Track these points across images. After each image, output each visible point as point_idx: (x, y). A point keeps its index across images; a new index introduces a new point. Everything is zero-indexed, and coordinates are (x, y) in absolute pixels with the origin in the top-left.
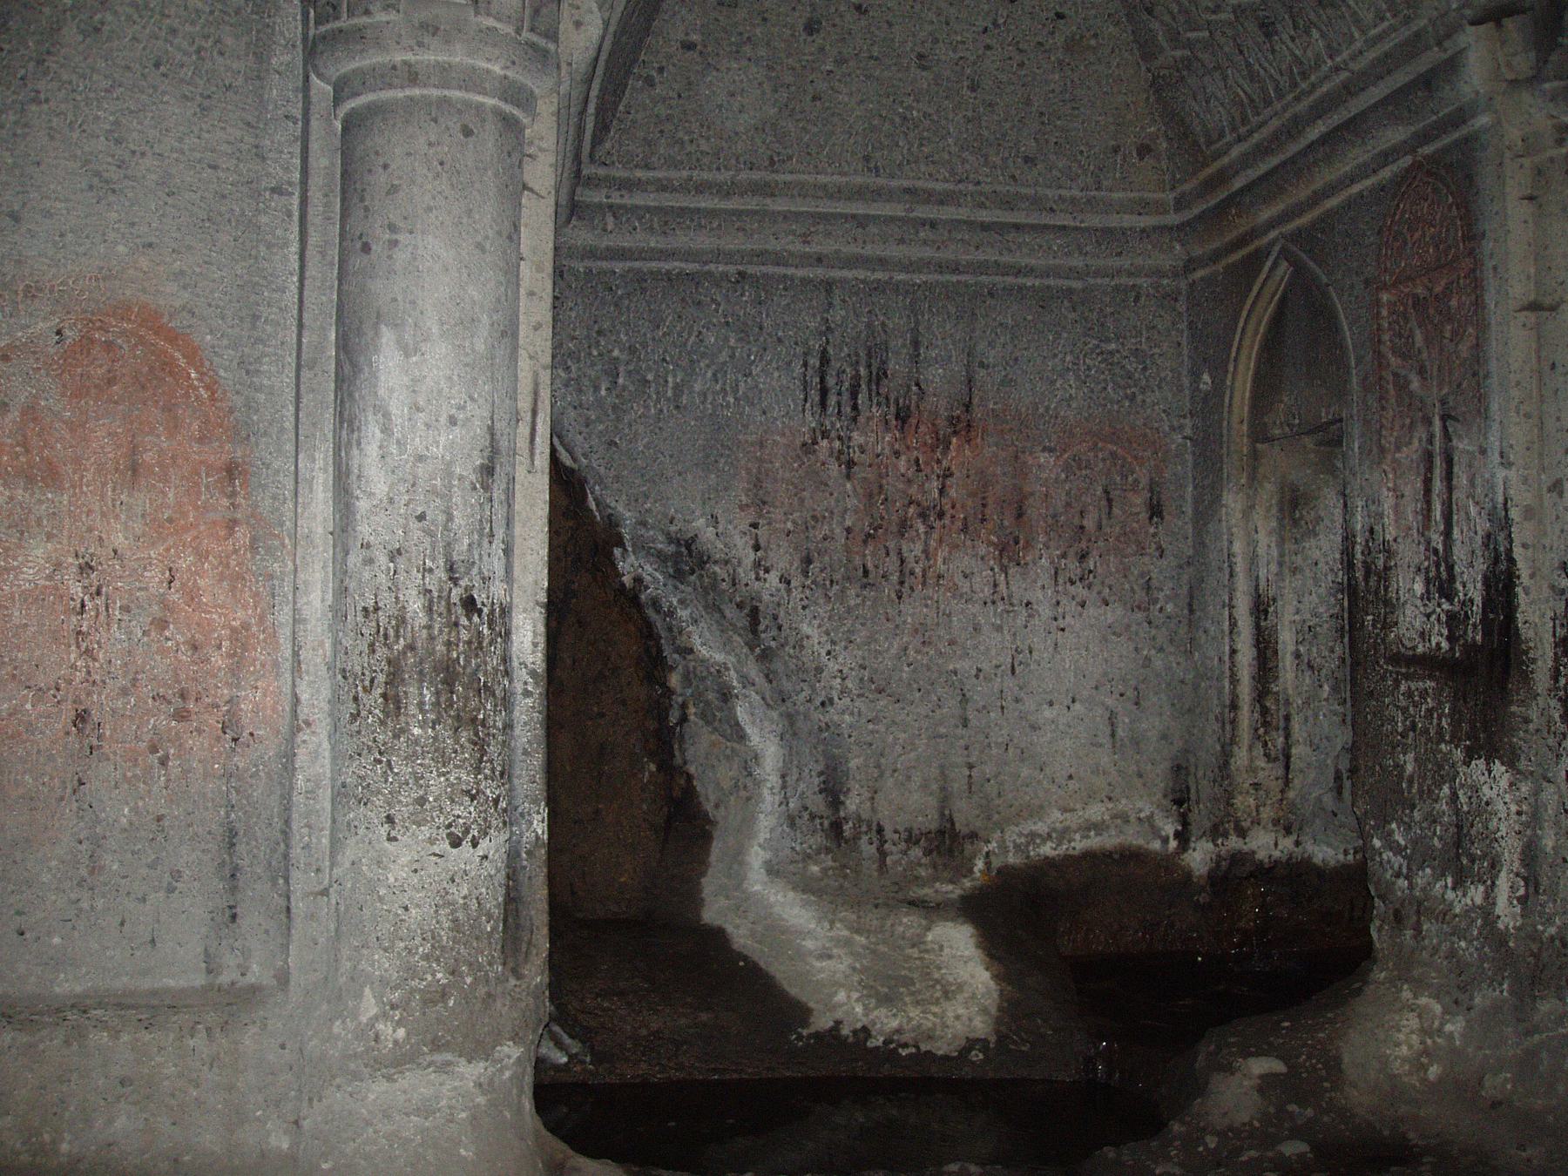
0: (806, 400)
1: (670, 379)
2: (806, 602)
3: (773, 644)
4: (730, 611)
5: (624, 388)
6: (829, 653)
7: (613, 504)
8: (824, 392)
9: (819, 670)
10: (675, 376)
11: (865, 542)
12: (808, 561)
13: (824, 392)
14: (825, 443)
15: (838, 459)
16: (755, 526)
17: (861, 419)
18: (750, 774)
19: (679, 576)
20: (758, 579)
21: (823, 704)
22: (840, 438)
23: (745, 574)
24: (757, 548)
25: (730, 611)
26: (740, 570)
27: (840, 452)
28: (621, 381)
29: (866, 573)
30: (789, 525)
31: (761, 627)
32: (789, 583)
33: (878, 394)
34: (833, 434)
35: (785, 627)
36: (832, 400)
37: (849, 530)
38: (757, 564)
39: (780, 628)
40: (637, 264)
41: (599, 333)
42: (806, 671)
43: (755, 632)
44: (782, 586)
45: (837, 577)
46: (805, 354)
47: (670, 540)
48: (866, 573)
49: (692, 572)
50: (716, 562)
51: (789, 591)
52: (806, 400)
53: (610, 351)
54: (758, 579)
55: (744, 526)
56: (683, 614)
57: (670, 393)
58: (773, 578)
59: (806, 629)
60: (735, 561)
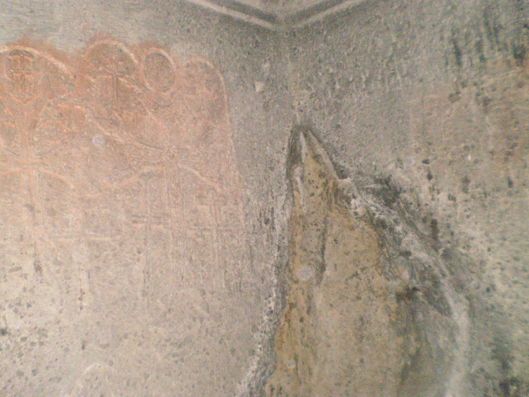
0: (447, 64)
1: (363, 76)
2: (468, 213)
3: (449, 245)
4: (420, 226)
5: (340, 90)
6: (489, 250)
7: (343, 164)
8: (458, 54)
9: (483, 263)
10: (364, 74)
11: (506, 160)
12: (466, 181)
13: (458, 54)
14: (465, 91)
15: (476, 100)
16: (426, 162)
17: (489, 64)
18: (454, 341)
19: (388, 203)
20: (433, 199)
21: (488, 290)
22: (475, 84)
23: (424, 195)
24: (430, 177)
25: (420, 226)
26: (422, 196)
27: (478, 95)
28: (338, 86)
29: (510, 184)
30: (449, 157)
31: (440, 235)
32: (454, 199)
33: (498, 42)
34: (470, 82)
35: (456, 231)
36: (465, 58)
37: (492, 152)
38: (432, 189)
39: (452, 234)
40: (328, 12)
41: (320, 61)
42: (474, 265)
43: (435, 238)
44: (451, 202)
45: (488, 190)
46: (441, 31)
47: (377, 181)
48: (510, 184)
49: (394, 201)
50: (405, 192)
51: (455, 206)
52: (447, 64)
53: (327, 70)
54: (433, 199)
55: (420, 164)
56: (399, 228)
57: (364, 86)
58: (443, 197)
59: (470, 232)
60: (417, 189)
